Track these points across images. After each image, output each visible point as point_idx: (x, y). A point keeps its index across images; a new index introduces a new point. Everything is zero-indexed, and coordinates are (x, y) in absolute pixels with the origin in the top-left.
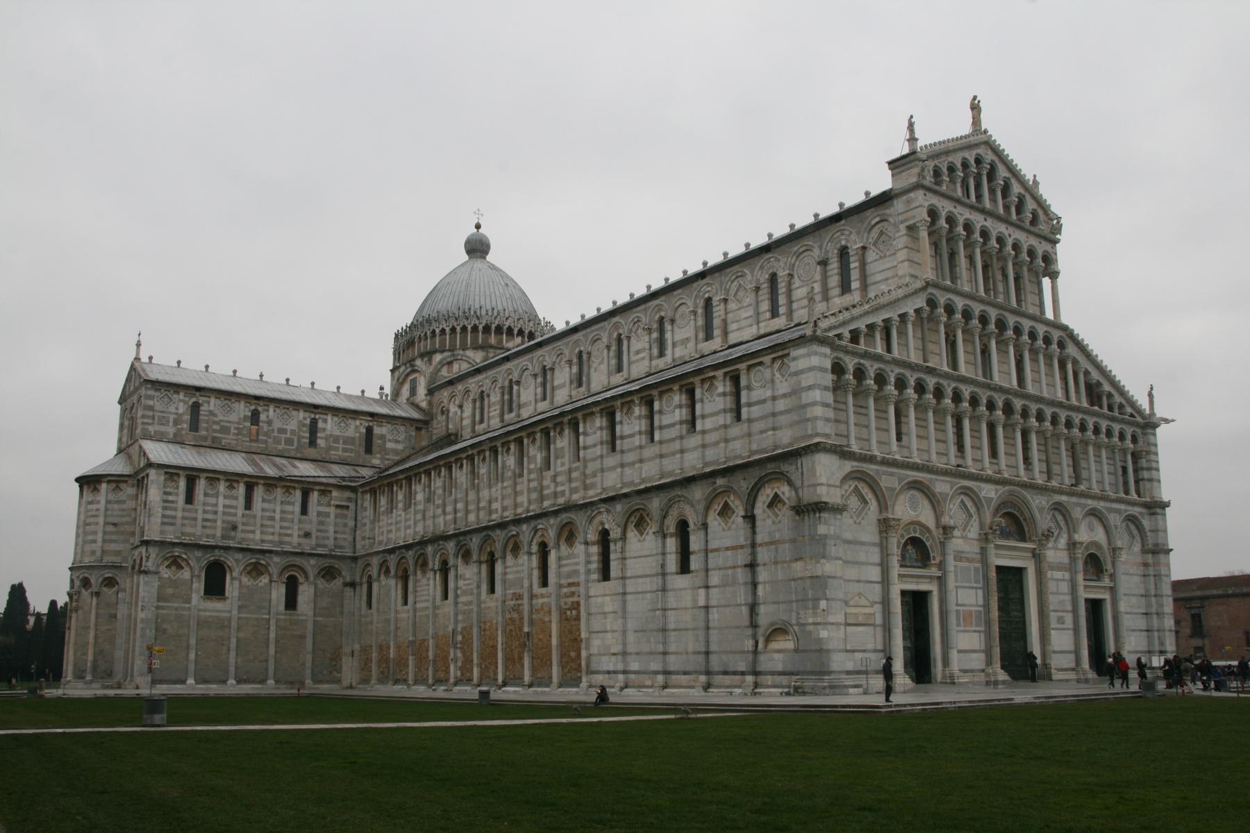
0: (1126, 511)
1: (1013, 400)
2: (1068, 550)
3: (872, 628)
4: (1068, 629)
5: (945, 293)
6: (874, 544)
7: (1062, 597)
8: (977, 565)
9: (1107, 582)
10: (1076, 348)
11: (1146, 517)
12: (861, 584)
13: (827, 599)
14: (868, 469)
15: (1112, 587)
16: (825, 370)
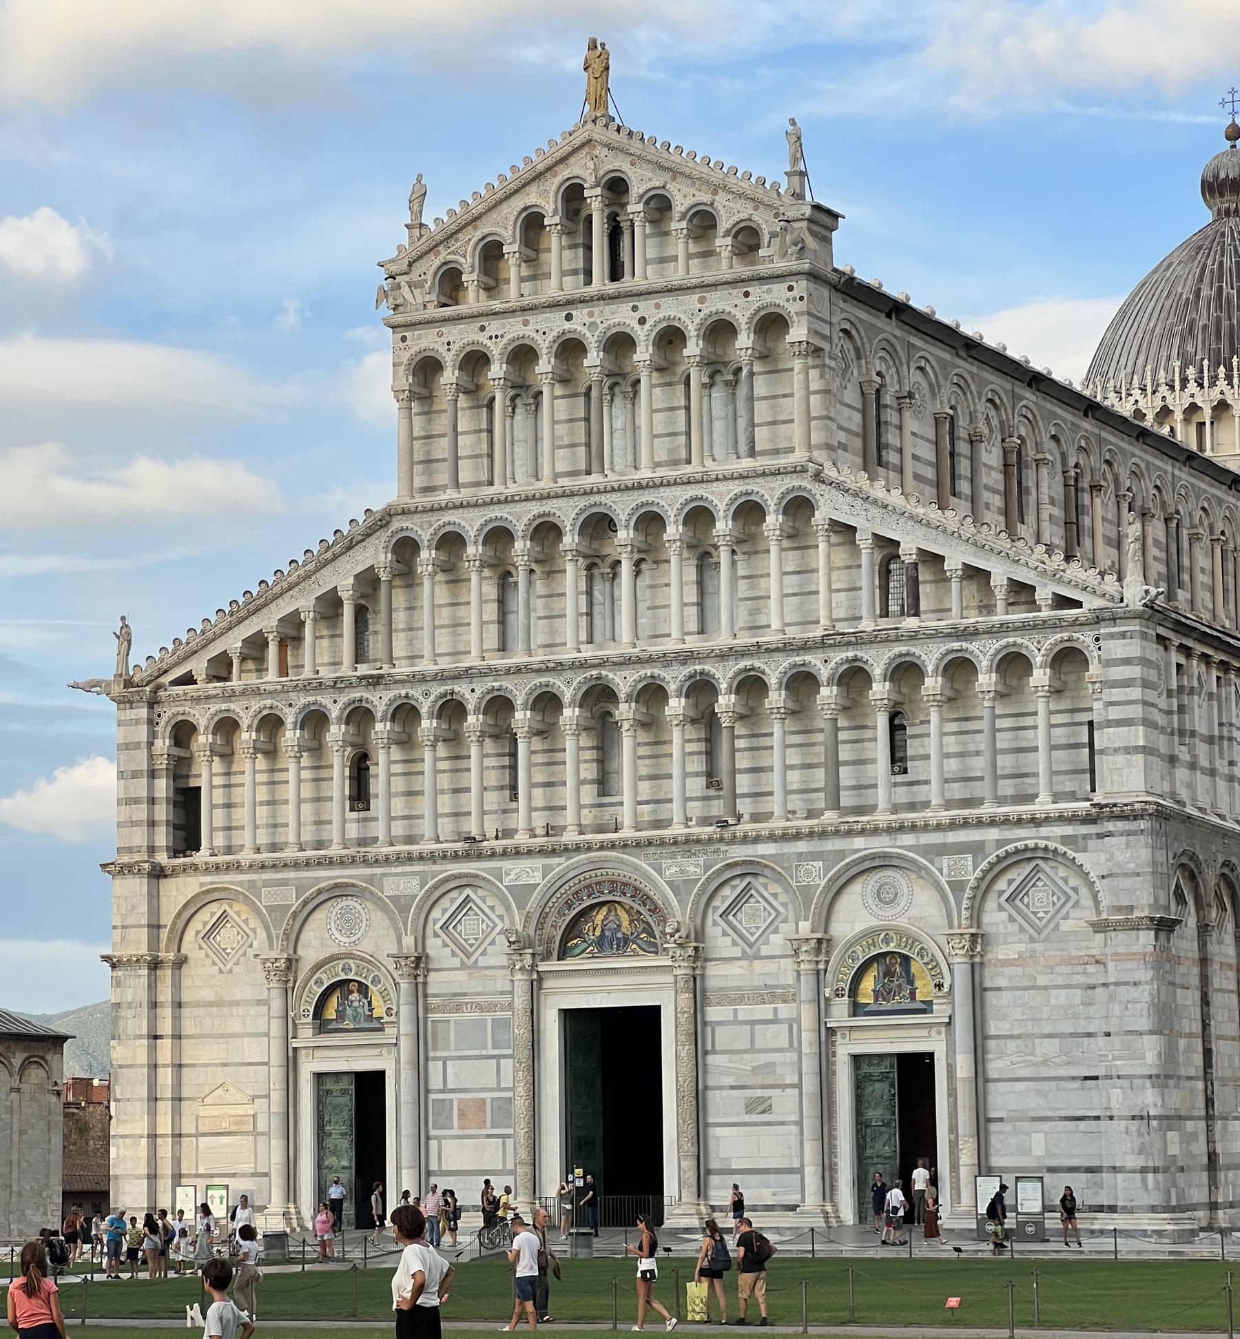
0: (1000, 843)
1: (611, 675)
2: (792, 956)
3: (251, 1138)
4: (782, 1123)
5: (432, 517)
6: (260, 1002)
7: (763, 1058)
8: (499, 1014)
9: (941, 1010)
10: (843, 500)
11: (1092, 844)
12: (232, 1069)
13: (115, 1100)
14: (233, 883)
15: (949, 1024)
16: (137, 745)
